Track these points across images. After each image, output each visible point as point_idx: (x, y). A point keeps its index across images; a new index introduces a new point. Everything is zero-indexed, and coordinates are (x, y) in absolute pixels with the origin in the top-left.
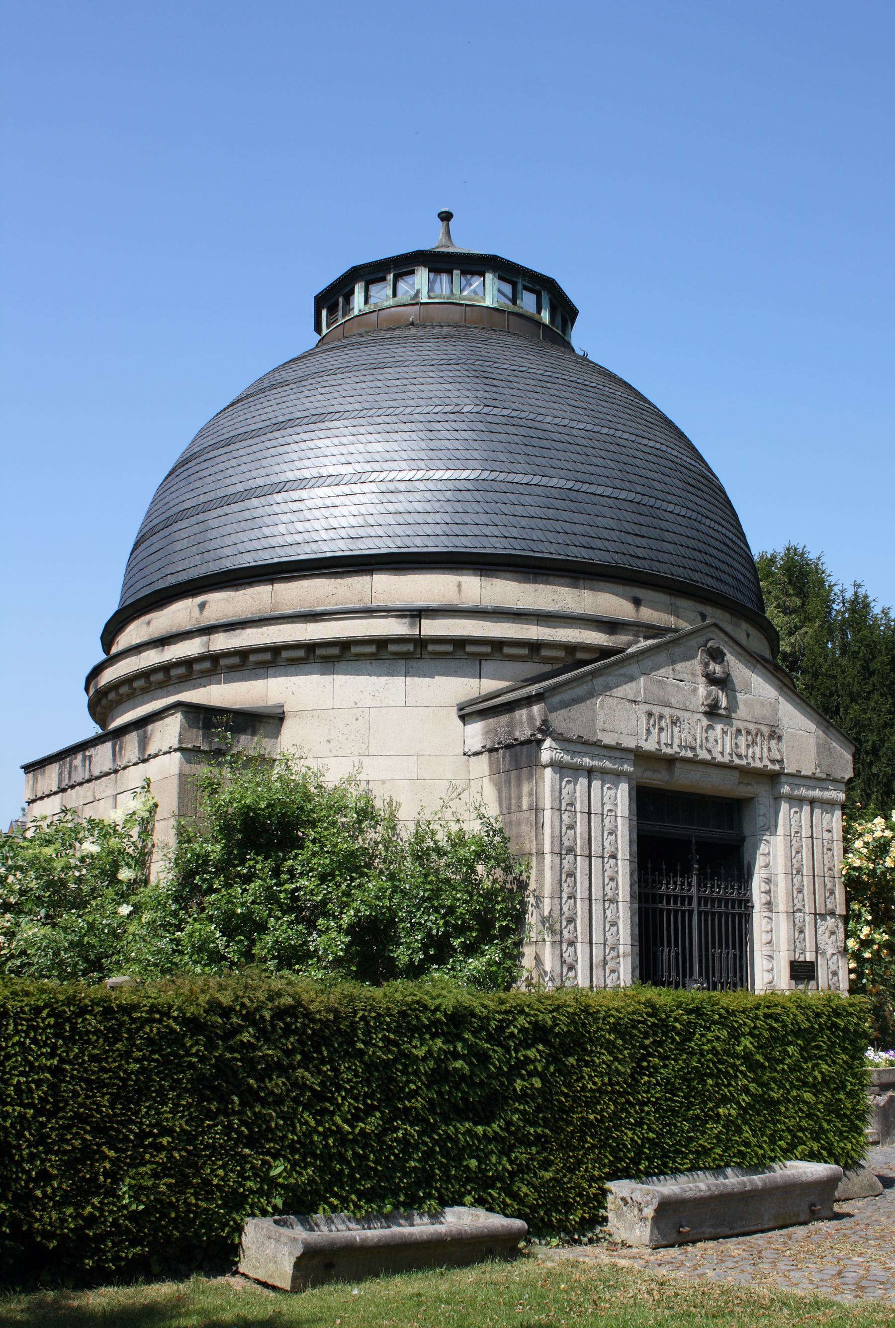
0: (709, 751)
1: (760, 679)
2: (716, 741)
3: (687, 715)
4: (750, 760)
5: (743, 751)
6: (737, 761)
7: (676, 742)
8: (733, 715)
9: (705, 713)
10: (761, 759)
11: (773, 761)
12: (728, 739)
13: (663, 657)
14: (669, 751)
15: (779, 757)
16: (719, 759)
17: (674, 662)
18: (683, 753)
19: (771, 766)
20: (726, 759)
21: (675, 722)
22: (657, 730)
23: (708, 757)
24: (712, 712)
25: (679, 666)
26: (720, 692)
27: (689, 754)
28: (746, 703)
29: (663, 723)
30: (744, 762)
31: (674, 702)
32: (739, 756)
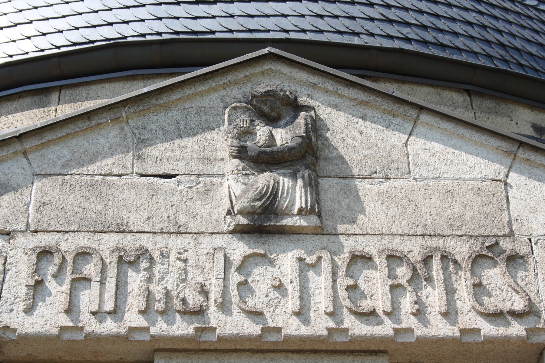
0: (255, 314)
1: (437, 146)
2: (279, 287)
3: (176, 243)
4: (408, 321)
5: (380, 302)
6: (358, 328)
7: (134, 302)
8: (341, 228)
9: (239, 231)
10: (450, 314)
11: (495, 316)
12: (320, 284)
13: (110, 134)
14: (109, 327)
15: (519, 305)
16: (292, 327)
17: (143, 142)
18: (160, 328)
19: (488, 329)
20: (319, 325)
21: (126, 261)
22: (66, 286)
23: (251, 328)
24: (262, 223)
25: (156, 150)
26: (285, 182)
27: (182, 328)
28: (386, 199)
29: (91, 269)
30: (387, 328)
31: (134, 219)
32: (370, 315)
